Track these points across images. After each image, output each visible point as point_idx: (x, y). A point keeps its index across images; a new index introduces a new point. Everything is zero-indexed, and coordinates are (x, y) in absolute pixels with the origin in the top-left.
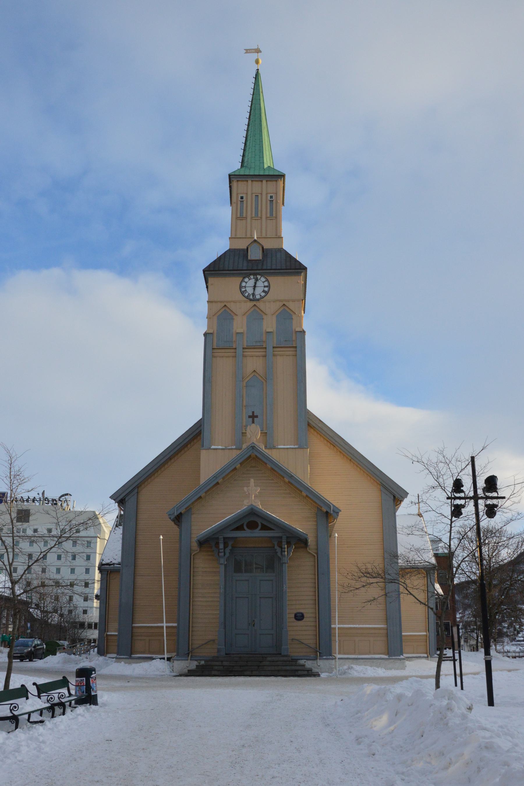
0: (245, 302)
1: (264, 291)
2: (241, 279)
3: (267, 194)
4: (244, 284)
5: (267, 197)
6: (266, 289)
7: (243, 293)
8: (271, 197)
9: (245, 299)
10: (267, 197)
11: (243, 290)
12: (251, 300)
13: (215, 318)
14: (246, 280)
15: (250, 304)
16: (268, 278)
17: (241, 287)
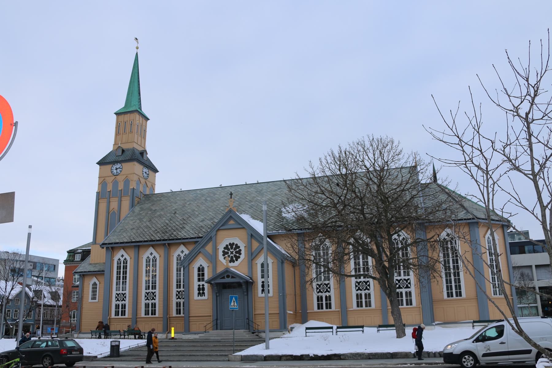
0: (112, 176)
1: (120, 171)
2: (111, 166)
3: (130, 121)
4: (112, 168)
5: (129, 122)
6: (121, 170)
7: (112, 172)
8: (132, 122)
9: (112, 175)
10: (129, 122)
11: (112, 171)
12: (115, 175)
13: (101, 185)
14: (114, 166)
15: (115, 177)
16: (122, 164)
17: (111, 169)
